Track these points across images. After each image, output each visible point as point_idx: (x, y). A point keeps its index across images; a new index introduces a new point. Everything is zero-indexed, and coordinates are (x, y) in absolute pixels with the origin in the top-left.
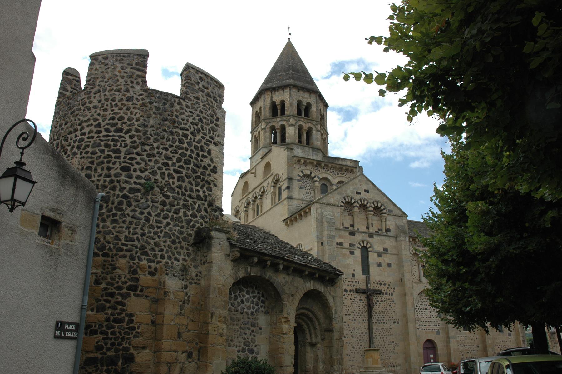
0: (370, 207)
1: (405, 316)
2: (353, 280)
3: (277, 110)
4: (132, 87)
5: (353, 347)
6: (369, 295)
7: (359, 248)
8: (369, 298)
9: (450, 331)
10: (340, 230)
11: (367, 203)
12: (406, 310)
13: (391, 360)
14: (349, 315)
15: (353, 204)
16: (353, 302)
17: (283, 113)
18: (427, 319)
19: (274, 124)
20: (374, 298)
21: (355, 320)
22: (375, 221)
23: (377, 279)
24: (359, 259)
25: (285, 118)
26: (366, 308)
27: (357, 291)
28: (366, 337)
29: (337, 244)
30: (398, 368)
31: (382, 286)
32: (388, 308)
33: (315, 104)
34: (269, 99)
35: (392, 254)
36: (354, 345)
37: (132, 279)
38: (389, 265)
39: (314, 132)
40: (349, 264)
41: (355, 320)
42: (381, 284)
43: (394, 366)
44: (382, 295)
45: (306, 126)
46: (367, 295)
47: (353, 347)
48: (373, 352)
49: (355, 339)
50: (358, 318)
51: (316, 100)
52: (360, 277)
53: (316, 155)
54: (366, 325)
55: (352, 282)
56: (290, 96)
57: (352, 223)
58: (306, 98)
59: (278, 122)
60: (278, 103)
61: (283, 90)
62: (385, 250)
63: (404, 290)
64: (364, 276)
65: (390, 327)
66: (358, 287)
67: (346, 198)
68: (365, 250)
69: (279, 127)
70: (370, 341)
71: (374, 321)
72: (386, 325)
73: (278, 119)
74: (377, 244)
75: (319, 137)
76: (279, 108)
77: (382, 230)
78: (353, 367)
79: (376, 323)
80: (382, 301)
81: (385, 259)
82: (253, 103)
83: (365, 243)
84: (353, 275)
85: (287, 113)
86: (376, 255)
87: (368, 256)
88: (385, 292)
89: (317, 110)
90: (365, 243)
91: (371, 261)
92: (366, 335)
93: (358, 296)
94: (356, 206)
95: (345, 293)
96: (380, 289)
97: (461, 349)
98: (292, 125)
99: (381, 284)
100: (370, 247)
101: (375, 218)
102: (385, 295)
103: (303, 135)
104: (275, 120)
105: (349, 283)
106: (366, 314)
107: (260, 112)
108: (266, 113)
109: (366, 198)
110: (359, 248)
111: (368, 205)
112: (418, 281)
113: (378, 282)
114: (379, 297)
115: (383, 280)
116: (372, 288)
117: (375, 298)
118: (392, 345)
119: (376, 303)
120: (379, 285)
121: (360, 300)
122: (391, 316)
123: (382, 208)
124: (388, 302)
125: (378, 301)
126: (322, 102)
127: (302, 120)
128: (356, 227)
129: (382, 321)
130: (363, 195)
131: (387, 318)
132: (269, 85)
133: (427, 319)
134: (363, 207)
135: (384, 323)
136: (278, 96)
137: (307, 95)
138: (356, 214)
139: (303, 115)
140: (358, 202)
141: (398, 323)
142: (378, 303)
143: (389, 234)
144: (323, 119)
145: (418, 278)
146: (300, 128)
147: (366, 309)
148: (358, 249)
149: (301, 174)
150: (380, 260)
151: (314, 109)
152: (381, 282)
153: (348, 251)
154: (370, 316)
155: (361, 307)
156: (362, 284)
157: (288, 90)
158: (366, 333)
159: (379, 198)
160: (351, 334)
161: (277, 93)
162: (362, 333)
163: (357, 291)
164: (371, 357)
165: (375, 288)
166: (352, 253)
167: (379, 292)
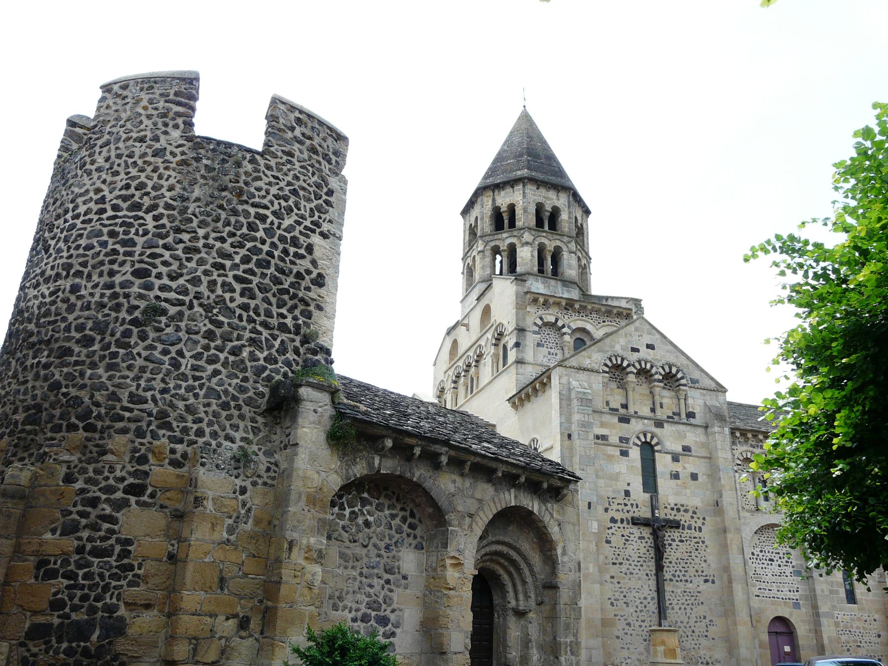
0: (656, 373)
1: (726, 569)
2: (626, 501)
3: (503, 220)
4: (166, 133)
5: (629, 624)
6: (658, 529)
7: (637, 445)
8: (654, 534)
9: (820, 604)
10: (601, 412)
11: (652, 367)
12: (728, 559)
13: (702, 652)
14: (621, 564)
15: (625, 368)
16: (627, 540)
17: (512, 224)
18: (774, 579)
19: (497, 243)
20: (667, 535)
22: (666, 397)
23: (672, 500)
24: (638, 464)
25: (515, 233)
26: (652, 552)
27: (636, 522)
28: (653, 607)
29: (598, 437)
31: (682, 513)
32: (693, 554)
33: (566, 209)
34: (490, 203)
35: (698, 457)
36: (630, 621)
37: (134, 474)
38: (694, 477)
39: (565, 255)
40: (618, 474)
41: (631, 573)
42: (678, 510)
44: (681, 530)
45: (550, 245)
46: (654, 530)
47: (629, 624)
48: (665, 634)
49: (631, 610)
50: (636, 571)
51: (569, 202)
52: (639, 495)
53: (568, 291)
54: (653, 583)
55: (626, 505)
56: (524, 197)
57: (624, 402)
58: (552, 199)
59: (505, 239)
60: (504, 209)
61: (513, 187)
62: (687, 449)
63: (723, 521)
64: (648, 495)
65: (699, 589)
66: (636, 515)
67: (613, 359)
68: (648, 450)
69: (505, 248)
70: (660, 612)
71: (667, 576)
73: (505, 235)
74: (671, 438)
75: (574, 262)
76: (506, 217)
77: (679, 414)
78: (628, 661)
79: (671, 580)
80: (682, 541)
81: (686, 465)
82: (465, 212)
83: (649, 436)
84: (627, 493)
85: (519, 224)
86: (669, 457)
87: (654, 461)
88: (686, 525)
89: (569, 218)
90: (649, 436)
91: (659, 468)
93: (636, 531)
94: (631, 372)
95: (612, 525)
96: (678, 518)
97: (843, 638)
98: (527, 243)
99: (678, 510)
100: (657, 444)
101: (666, 393)
102: (686, 531)
103: (546, 259)
104: (499, 236)
106: (652, 564)
107: (476, 226)
108: (486, 226)
109: (649, 358)
110: (637, 445)
111: (653, 371)
112: (753, 508)
113: (673, 506)
114: (676, 534)
115: (684, 502)
116: (662, 516)
117: (670, 535)
118: (703, 624)
119: (670, 545)
120: (675, 512)
121: (640, 538)
122: (700, 570)
123: (679, 375)
124: (692, 543)
125: (673, 540)
126: (579, 206)
127: (544, 234)
128: (631, 410)
129: (682, 577)
130: (644, 353)
131: (691, 571)
132: (490, 181)
133: (774, 579)
134: (644, 373)
135: (686, 581)
136: (504, 197)
137: (552, 194)
138: (632, 385)
139: (546, 228)
140: (634, 366)
141: (713, 582)
142: (674, 544)
143: (692, 421)
144: (580, 233)
145: (753, 502)
146: (541, 250)
147: (653, 555)
148: (635, 447)
149: (540, 322)
150: (677, 467)
151: (564, 216)
153: (618, 449)
154: (659, 568)
156: (644, 509)
157: (521, 187)
158: (653, 599)
159: (672, 359)
160: (625, 600)
161: (503, 193)
162: (645, 598)
163: (635, 522)
164: (663, 643)
165: (669, 517)
166: (624, 453)
167: (675, 525)
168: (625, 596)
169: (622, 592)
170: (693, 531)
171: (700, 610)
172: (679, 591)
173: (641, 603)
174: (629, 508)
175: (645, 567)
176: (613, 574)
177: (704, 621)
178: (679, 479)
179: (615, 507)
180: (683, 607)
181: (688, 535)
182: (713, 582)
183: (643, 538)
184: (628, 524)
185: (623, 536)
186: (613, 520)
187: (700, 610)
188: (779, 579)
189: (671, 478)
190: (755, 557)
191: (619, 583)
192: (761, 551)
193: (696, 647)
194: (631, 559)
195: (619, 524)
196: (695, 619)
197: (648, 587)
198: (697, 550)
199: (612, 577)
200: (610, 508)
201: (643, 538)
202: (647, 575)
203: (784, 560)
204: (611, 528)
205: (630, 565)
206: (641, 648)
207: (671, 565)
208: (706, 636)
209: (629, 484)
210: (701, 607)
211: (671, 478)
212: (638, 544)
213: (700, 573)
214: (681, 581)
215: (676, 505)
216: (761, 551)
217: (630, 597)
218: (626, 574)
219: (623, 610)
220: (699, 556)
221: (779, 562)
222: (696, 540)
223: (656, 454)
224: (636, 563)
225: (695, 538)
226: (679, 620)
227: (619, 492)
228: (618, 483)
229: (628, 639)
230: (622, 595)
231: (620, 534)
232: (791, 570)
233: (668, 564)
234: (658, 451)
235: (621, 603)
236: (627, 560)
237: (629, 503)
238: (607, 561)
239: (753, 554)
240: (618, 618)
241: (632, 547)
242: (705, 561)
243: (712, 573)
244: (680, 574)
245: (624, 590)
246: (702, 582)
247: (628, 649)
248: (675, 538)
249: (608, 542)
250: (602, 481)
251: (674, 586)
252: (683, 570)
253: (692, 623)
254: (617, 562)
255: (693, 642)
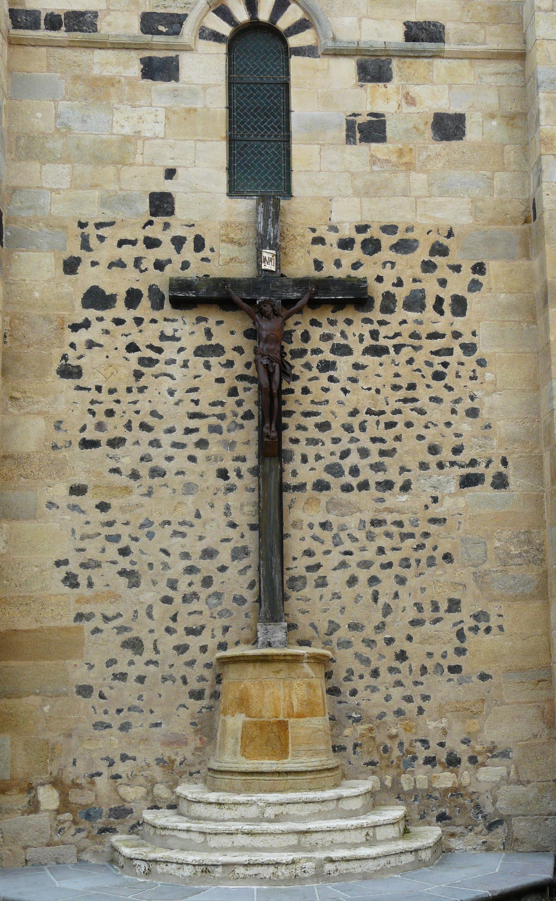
2: (155, 232)
5: (135, 645)
6: (272, 316)
13: (431, 726)
16: (150, 362)
20: (316, 333)
21: (156, 473)
23: (347, 215)
24: (217, 102)
26: (249, 397)
27: (186, 297)
30: (491, 773)
31: (386, 254)
32: (422, 394)
35: (472, 57)
36: (139, 631)
38: (448, 127)
41: (156, 473)
43: (453, 762)
44: (376, 315)
47: (135, 645)
49: (148, 594)
54: (243, 502)
55: (152, 243)
65: (436, 511)
72: (396, 499)
79: (321, 486)
80: (377, 351)
81: (415, 90)
84: (162, 204)
86: (348, 68)
88: (401, 294)
91: (303, 107)
92: (235, 567)
93: (188, 329)
95: (92, 314)
99: (372, 246)
100: (300, 26)
102: (400, 313)
105: (127, 254)
113: (347, 232)
114: (354, 329)
120: (357, 253)
121: (200, 351)
124: (421, 357)
129: (366, 474)
131: (411, 451)
135: (388, 485)
141: (501, 482)
142: (344, 365)
147: (250, 405)
152: (374, 232)
154: (271, 451)
155: (211, 392)
156: (226, 251)
158: (238, 553)
160: (124, 563)
162: (209, 554)
163: (186, 297)
168: (125, 552)
169: (116, 538)
170: (430, 312)
171: (439, 583)
172: (352, 522)
173: (191, 570)
174: (166, 251)
175: (214, 449)
176: (81, 479)
177: (455, 617)
178: (382, 139)
179: (106, 252)
180: (363, 575)
181: (405, 330)
182: (501, 482)
183: (218, 350)
184: (158, 305)
185: (132, 348)
186: (96, 298)
187: (439, 583)
189: (350, 138)
191: (103, 507)
193: (410, 708)
194: (159, 426)
195: (120, 310)
196: (412, 614)
197: (222, 517)
198: (438, 376)
199: (78, 490)
200: (87, 257)
201: (218, 350)
202: (223, 474)
204: (86, 324)
205: (156, 443)
206: (180, 722)
207: (325, 436)
208: (455, 669)
209: (170, 173)
210: (443, 573)
211: (350, 138)
212: (195, 372)
213: (446, 455)
214: (364, 486)
215: (362, 229)
217: (146, 552)
218: (135, 475)
219: (115, 597)
220: (448, 397)
222: (437, 344)
223: (295, 61)
224: (178, 436)
225: (434, 336)
226: (343, 621)
227: (126, 201)
228: (127, 173)
229: (128, 692)
230: (112, 549)
231: (124, 342)
233: (315, 433)
234: (299, 51)
235: (108, 577)
236: (144, 427)
237: (165, 238)
238: (60, 438)
240: (88, 626)
241: (167, 383)
242: (473, 413)
243: (497, 453)
244: (363, 464)
245: (125, 532)
246: (453, 486)
247: (125, 727)
248: (352, 342)
249: (69, 372)
250: (64, 169)
251: (332, 506)
252: (374, 448)
253: (398, 626)
254: (103, 437)
255: (397, 693)
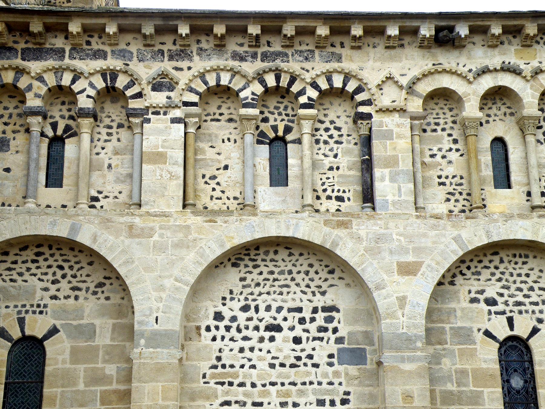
18: (274, 375)
133: (274, 375)
188: (292, 374)
190: (226, 322)
192: (246, 308)
203: (313, 327)
216: (246, 308)
221: (298, 331)
232: (333, 348)
239: (218, 316)
